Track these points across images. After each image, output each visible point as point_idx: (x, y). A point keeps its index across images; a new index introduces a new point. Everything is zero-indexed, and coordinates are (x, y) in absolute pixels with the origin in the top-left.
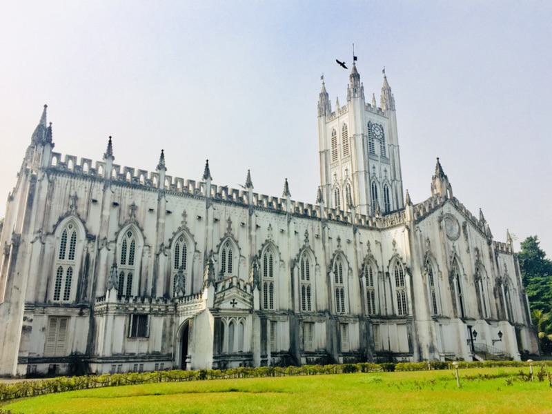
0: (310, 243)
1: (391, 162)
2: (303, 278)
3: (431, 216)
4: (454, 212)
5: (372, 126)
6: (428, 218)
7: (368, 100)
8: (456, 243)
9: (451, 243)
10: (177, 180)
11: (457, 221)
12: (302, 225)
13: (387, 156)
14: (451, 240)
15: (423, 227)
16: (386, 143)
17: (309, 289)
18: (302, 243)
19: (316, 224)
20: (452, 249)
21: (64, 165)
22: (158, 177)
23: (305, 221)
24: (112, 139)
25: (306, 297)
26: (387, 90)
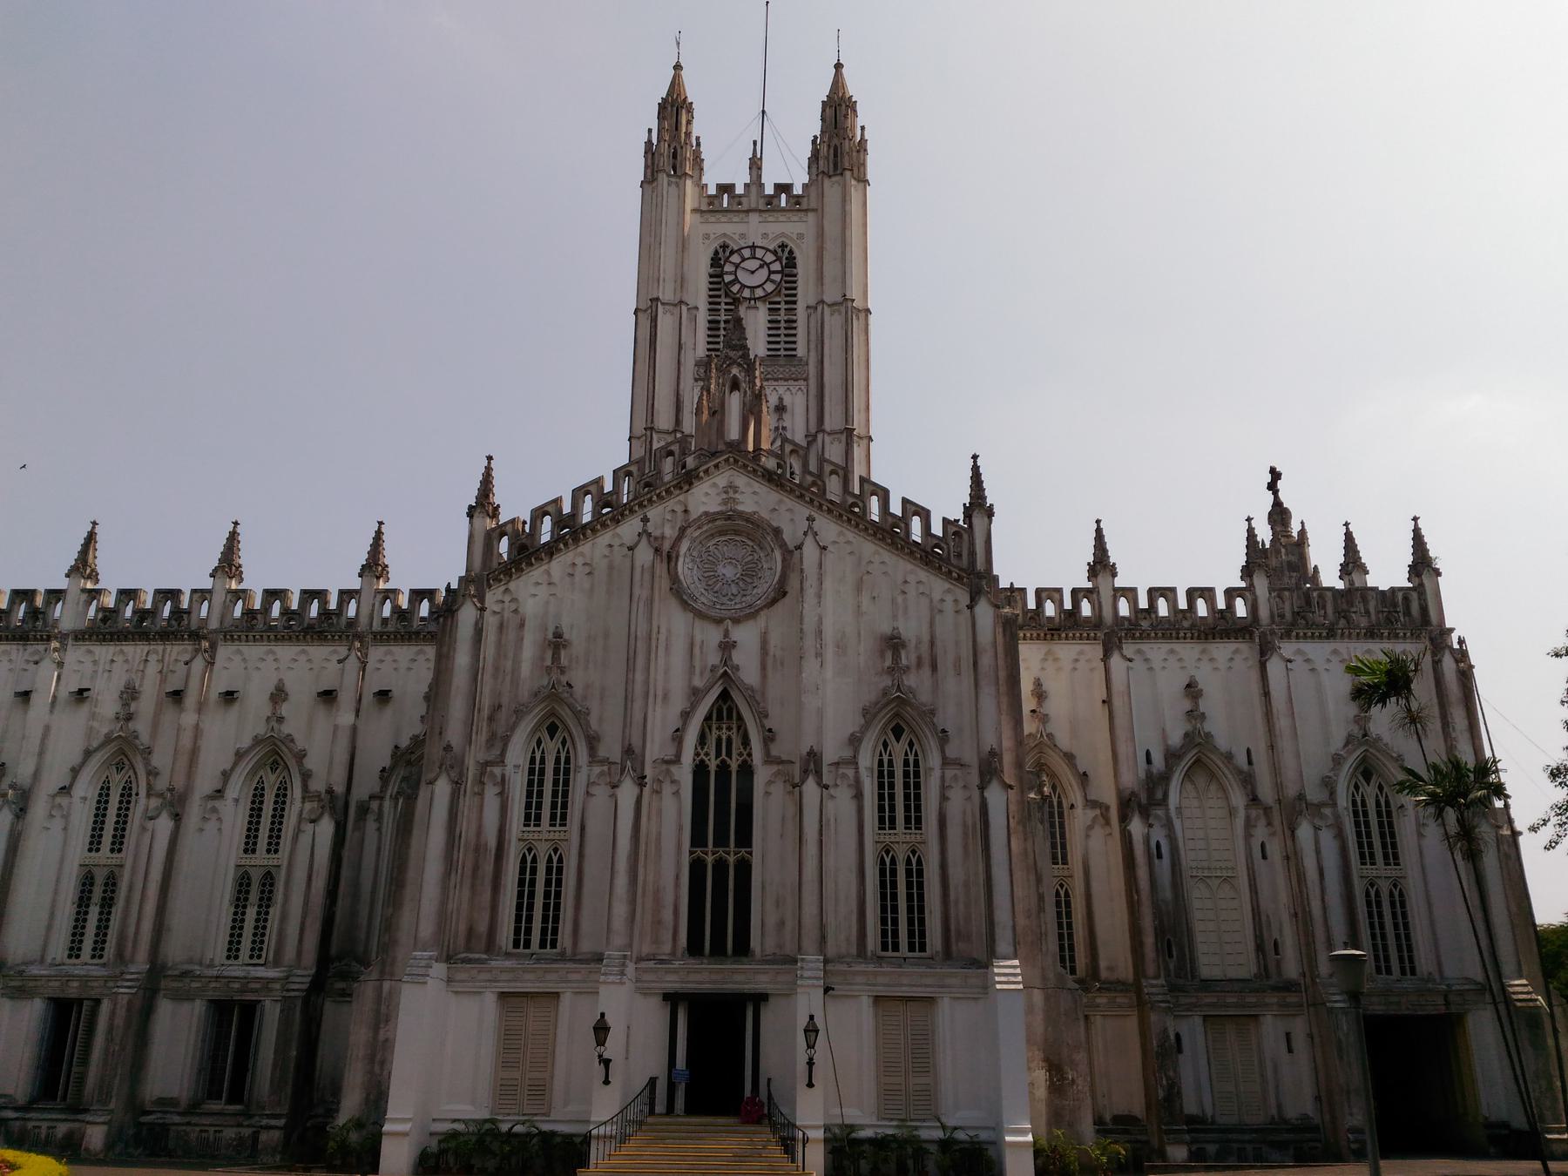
0: (141, 726)
1: (812, 370)
2: (1366, 857)
3: (604, 538)
4: (754, 498)
5: (727, 260)
6: (585, 547)
7: (712, 179)
8: (746, 636)
9: (711, 636)
10: (1154, 593)
11: (777, 532)
12: (108, 669)
13: (801, 352)
14: (719, 621)
15: (543, 591)
16: (801, 307)
17: (111, 883)
18: (105, 730)
19: (177, 651)
20: (714, 658)
21: (152, 613)
22: (1057, 596)
23: (135, 651)
24: (384, 529)
25: (94, 912)
26: (838, 109)
